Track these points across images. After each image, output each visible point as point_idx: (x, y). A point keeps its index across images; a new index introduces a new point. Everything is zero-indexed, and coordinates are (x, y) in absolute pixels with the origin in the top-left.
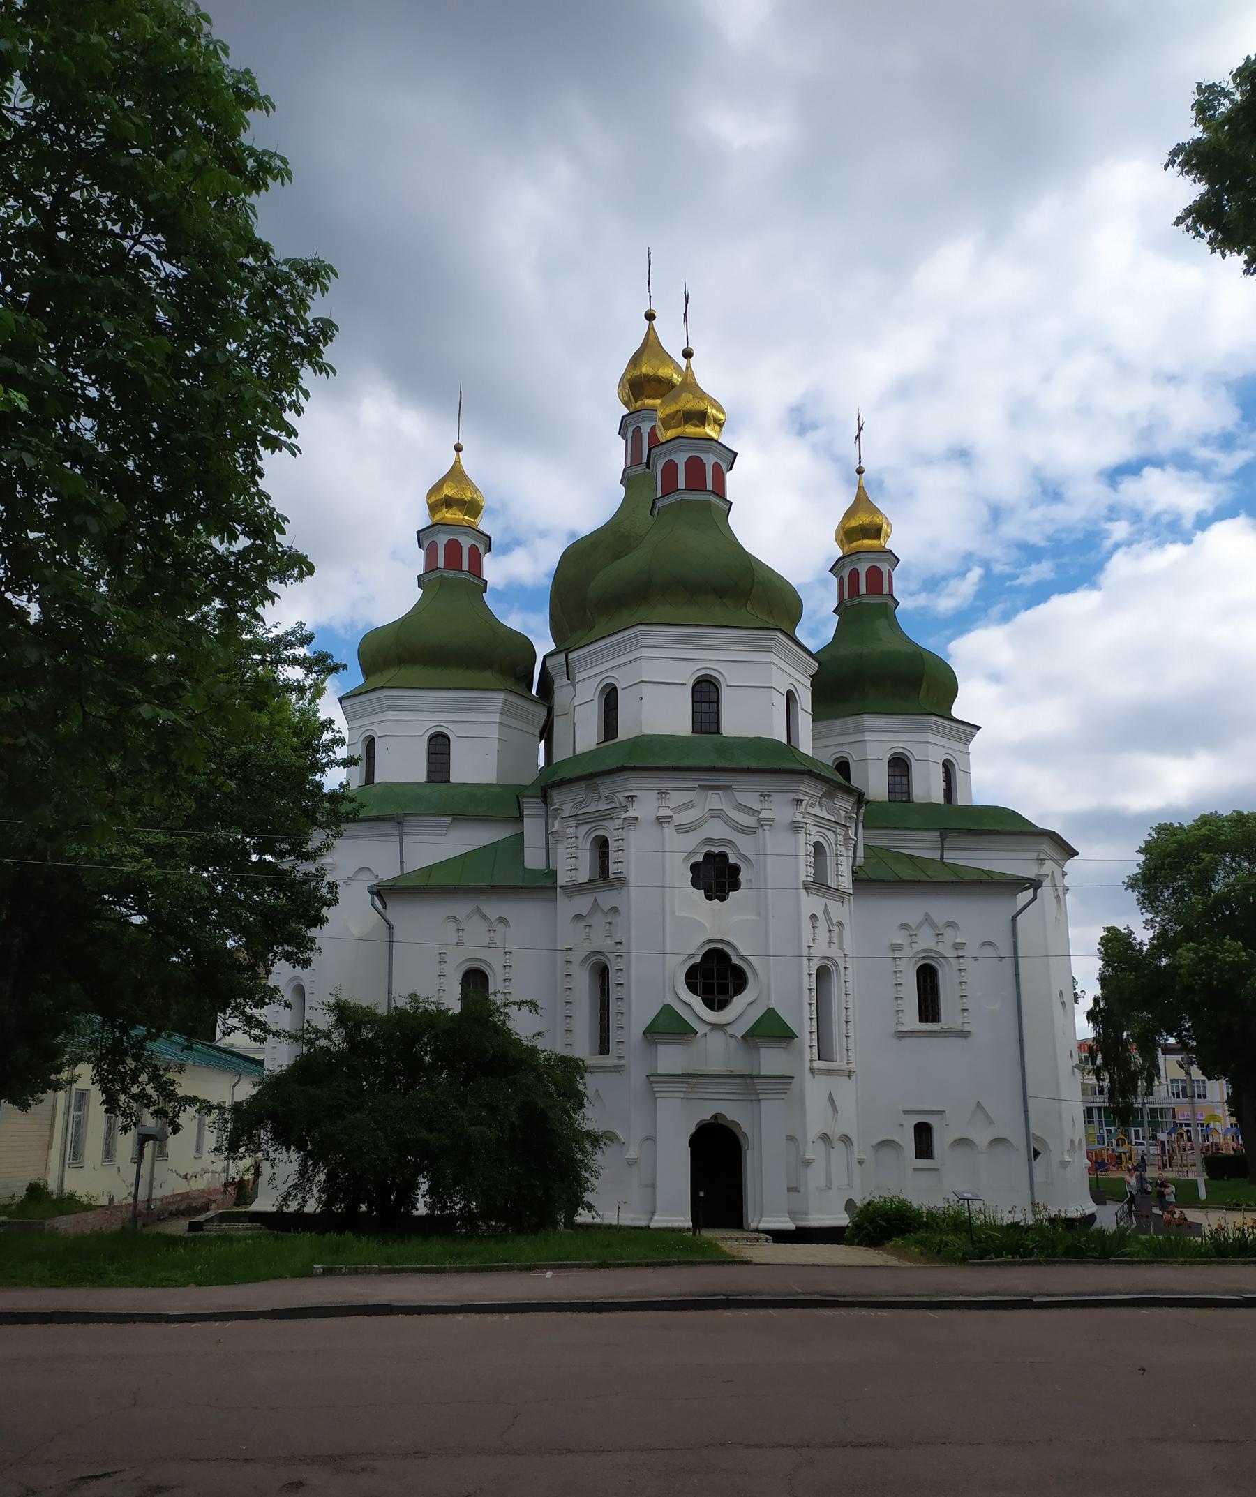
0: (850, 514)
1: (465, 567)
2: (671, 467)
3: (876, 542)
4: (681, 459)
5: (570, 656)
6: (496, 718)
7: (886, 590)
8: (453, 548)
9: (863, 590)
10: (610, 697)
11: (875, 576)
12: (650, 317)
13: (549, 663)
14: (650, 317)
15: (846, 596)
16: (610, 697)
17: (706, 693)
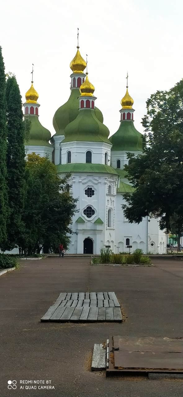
0: (124, 98)
1: (35, 113)
2: (82, 102)
3: (130, 107)
4: (85, 100)
5: (61, 144)
6: (43, 151)
7: (131, 118)
8: (32, 109)
9: (126, 119)
10: (69, 154)
11: (129, 115)
12: (78, 48)
13: (54, 137)
14: (78, 48)
15: (122, 119)
16: (69, 154)
17: (89, 154)
